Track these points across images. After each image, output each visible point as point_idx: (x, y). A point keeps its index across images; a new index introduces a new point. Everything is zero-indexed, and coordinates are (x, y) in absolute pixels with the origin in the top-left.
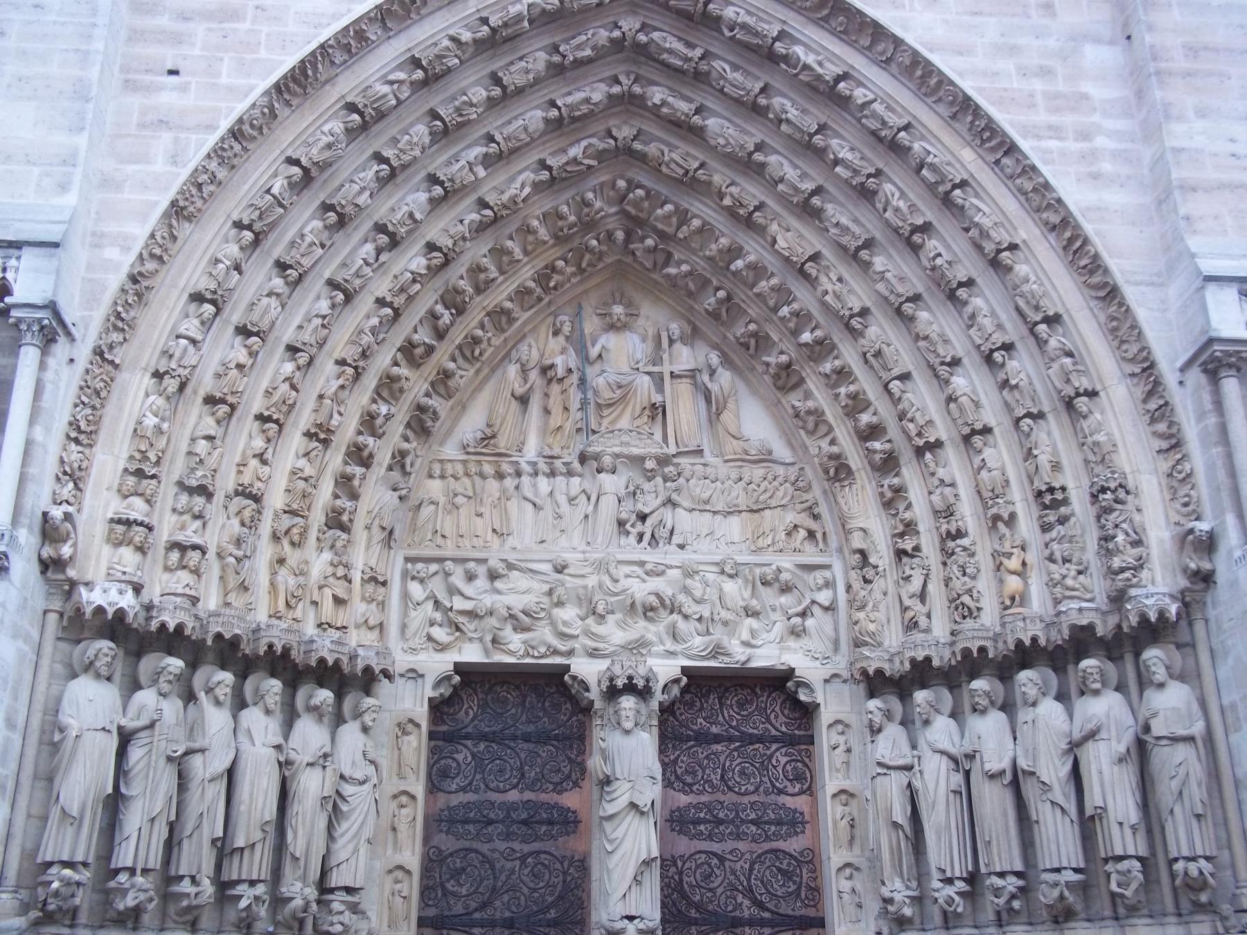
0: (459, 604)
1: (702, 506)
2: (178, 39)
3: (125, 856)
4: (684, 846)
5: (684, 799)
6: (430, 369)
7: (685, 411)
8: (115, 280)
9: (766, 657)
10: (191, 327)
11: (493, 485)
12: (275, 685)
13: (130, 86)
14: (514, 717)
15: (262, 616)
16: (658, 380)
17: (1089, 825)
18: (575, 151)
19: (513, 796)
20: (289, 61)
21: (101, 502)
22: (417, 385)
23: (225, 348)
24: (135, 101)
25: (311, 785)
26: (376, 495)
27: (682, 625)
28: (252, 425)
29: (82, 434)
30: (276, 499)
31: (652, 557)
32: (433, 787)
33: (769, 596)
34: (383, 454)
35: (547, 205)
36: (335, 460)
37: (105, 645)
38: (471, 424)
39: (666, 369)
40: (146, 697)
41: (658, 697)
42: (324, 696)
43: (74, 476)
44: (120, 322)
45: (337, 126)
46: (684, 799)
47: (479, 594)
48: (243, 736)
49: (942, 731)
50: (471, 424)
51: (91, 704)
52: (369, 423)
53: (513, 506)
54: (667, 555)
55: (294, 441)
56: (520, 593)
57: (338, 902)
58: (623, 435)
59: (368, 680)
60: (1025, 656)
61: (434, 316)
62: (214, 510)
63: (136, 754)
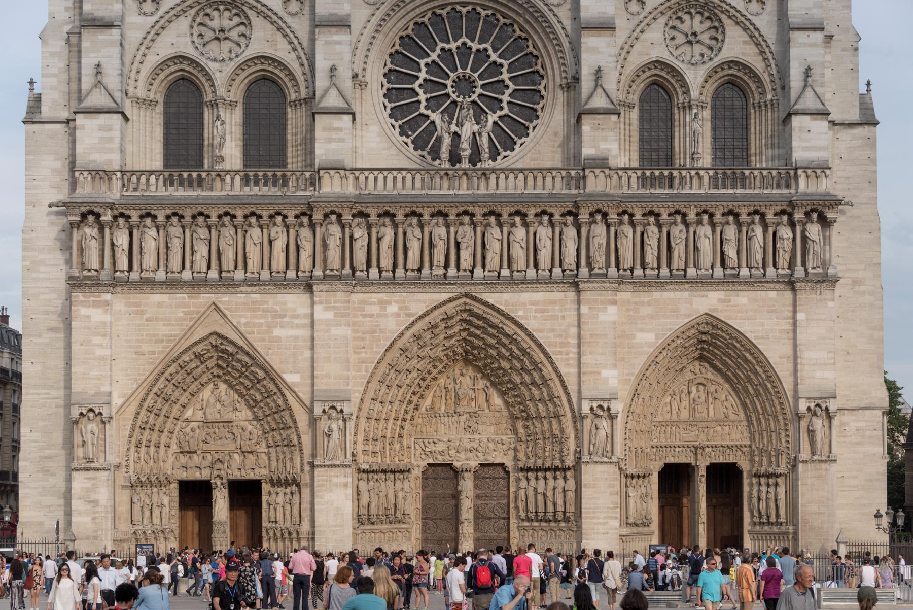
0: (427, 449)
1: (484, 424)
2: (363, 339)
3: (372, 512)
4: (479, 502)
5: (479, 492)
6: (418, 395)
7: (482, 397)
8: (358, 401)
9: (497, 461)
10: (372, 407)
11: (434, 419)
12: (392, 476)
13: (355, 353)
14: (442, 476)
15: (388, 462)
16: (474, 389)
17: (555, 505)
18: (452, 342)
19: (441, 491)
20: (388, 344)
21: (360, 447)
22: (415, 399)
23: (378, 406)
24: (357, 356)
25: (400, 495)
26: (407, 425)
27: (479, 455)
28: (383, 421)
29: (356, 434)
30: (389, 435)
31: (472, 437)
32: (423, 490)
33: (499, 445)
34: (408, 417)
35: (445, 352)
36: (399, 422)
37: (364, 476)
38: (428, 402)
39: (476, 387)
40: (371, 483)
41: (473, 470)
42: (401, 476)
43: (355, 443)
44: (360, 409)
45: (398, 355)
46: (479, 492)
47: (431, 447)
48: (387, 487)
49: (533, 482)
50: (428, 402)
51: (363, 486)
52: (406, 412)
53: (439, 425)
54: (477, 437)
55: (391, 421)
56: (441, 447)
57: (406, 516)
58: (464, 407)
59: (409, 471)
60: (548, 469)
61: (419, 384)
62: (379, 443)
63: (372, 494)
